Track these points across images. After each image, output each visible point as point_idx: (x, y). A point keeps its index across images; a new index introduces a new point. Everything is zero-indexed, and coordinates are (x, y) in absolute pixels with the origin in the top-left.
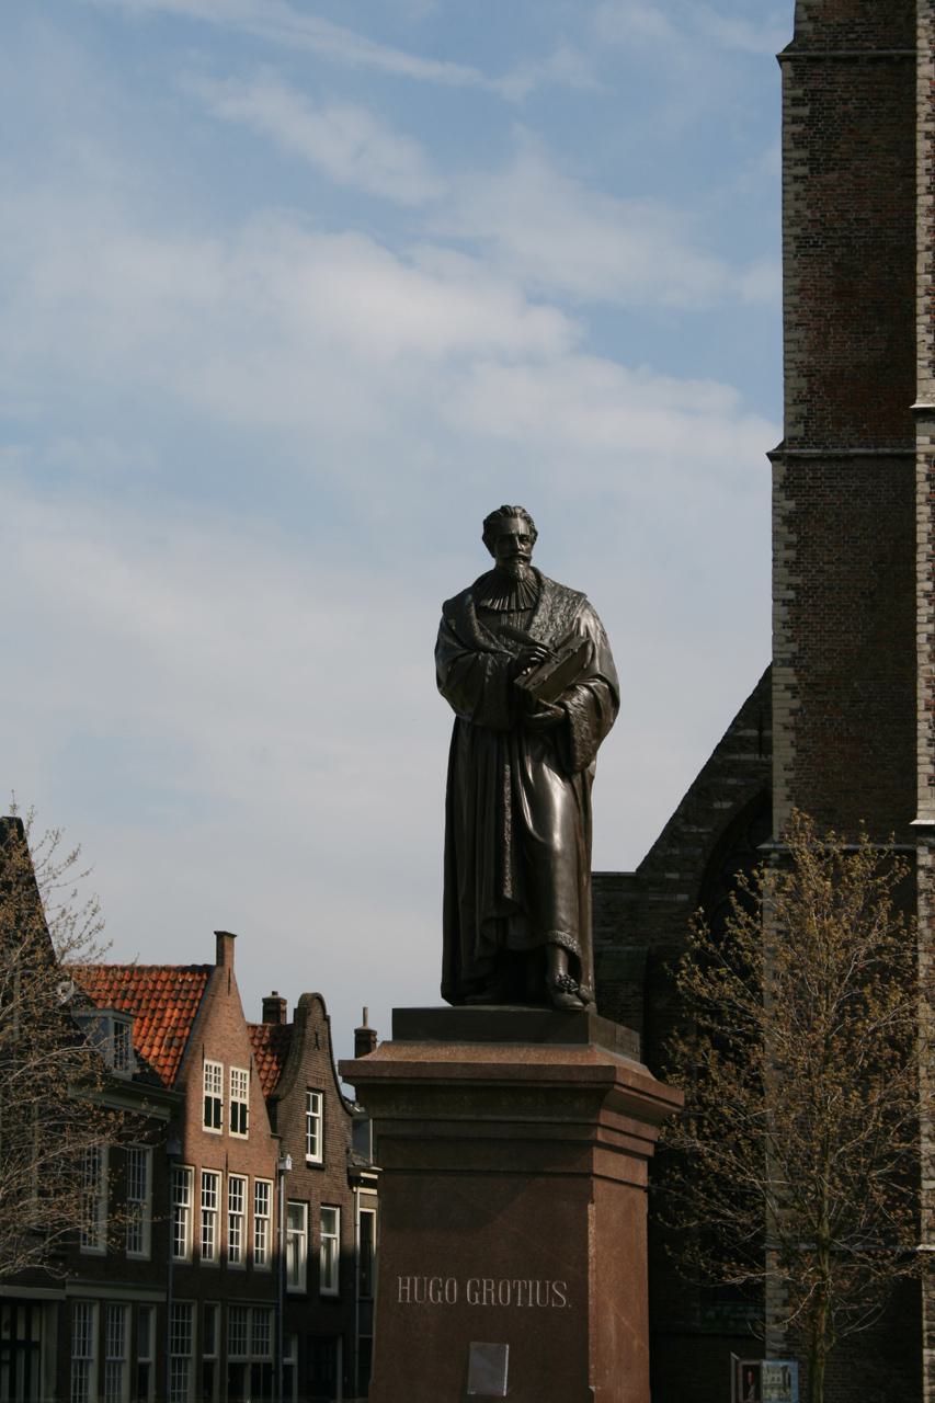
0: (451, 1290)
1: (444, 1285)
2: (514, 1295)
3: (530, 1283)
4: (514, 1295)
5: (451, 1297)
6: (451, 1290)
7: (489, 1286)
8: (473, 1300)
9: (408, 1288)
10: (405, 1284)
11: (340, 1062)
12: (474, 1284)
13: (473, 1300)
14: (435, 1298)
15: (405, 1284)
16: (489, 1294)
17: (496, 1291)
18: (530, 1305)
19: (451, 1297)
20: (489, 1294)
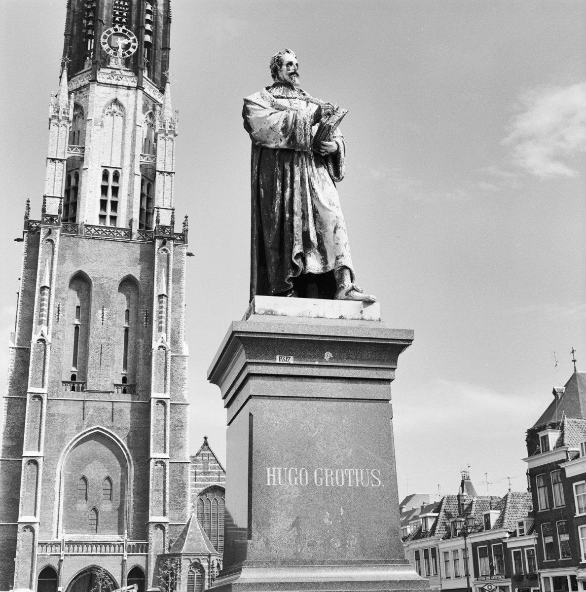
0: (304, 477)
1: (298, 473)
2: (346, 479)
3: (357, 471)
4: (346, 479)
5: (304, 482)
6: (304, 477)
7: (329, 472)
8: (319, 483)
9: (274, 476)
10: (271, 473)
11: (72, 380)
12: (319, 472)
13: (319, 483)
14: (293, 482)
15: (271, 473)
16: (329, 479)
17: (334, 476)
18: (357, 485)
19: (304, 482)
20: (329, 479)
